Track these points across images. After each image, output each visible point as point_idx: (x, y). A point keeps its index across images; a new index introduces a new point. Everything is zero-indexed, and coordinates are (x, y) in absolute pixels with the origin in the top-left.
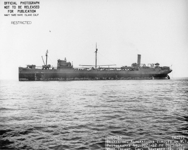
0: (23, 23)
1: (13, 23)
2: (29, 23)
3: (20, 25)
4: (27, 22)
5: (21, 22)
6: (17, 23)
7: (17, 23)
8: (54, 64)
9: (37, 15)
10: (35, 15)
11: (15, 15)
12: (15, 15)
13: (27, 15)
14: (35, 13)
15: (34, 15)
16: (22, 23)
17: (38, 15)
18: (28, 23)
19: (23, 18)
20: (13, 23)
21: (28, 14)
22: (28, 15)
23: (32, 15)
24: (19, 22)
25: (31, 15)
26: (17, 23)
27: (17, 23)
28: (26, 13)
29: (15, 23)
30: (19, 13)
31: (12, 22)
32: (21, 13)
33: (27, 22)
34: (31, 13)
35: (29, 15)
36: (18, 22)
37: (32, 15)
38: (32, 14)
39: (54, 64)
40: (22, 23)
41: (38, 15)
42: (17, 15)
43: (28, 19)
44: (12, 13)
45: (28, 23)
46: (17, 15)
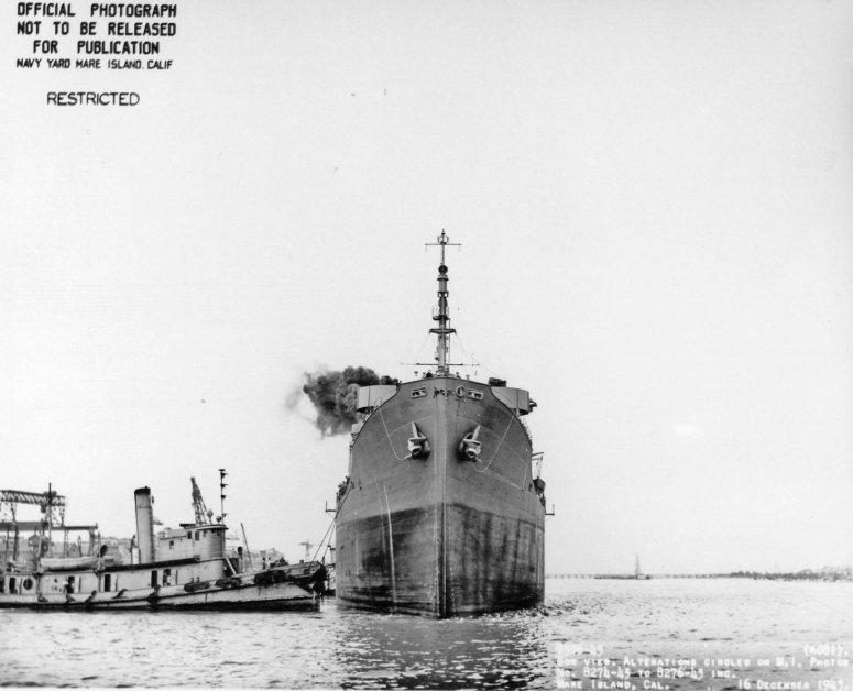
0: (100, 100)
1: (56, 98)
2: (126, 100)
4: (117, 97)
6: (73, 101)
7: (74, 98)
9: (163, 65)
10: (157, 65)
11: (64, 63)
12: (64, 63)
14: (155, 57)
15: (152, 65)
16: (97, 99)
17: (169, 64)
19: (103, 79)
20: (56, 98)
21: (123, 58)
22: (122, 64)
23: (144, 64)
24: (84, 97)
25: (136, 65)
26: (74, 98)
27: (73, 101)
28: (113, 56)
29: (66, 99)
30: (84, 56)
32: (93, 56)
33: (117, 97)
35: (127, 65)
36: (78, 97)
37: (144, 64)
40: (97, 99)
41: (169, 64)
42: (73, 63)
46: (73, 63)
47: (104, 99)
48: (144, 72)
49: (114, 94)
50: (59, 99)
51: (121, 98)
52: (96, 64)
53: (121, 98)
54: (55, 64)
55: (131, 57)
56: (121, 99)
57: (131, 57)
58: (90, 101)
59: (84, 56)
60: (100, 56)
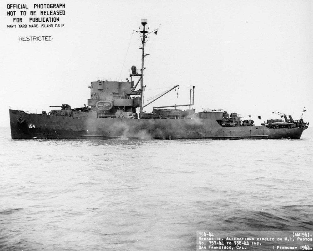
2: (48, 38)
4: (44, 38)
5: (35, 38)
10: (59, 26)
11: (24, 26)
12: (24, 26)
13: (44, 27)
14: (58, 23)
15: (57, 26)
16: (37, 39)
17: (63, 25)
18: (46, 39)
19: (39, 31)
22: (46, 26)
23: (54, 26)
24: (32, 38)
25: (51, 26)
28: (43, 23)
29: (25, 39)
30: (32, 23)
31: (20, 38)
32: (36, 23)
34: (52, 23)
35: (47, 26)
37: (54, 26)
38: (54, 23)
40: (37, 39)
41: (63, 25)
42: (28, 26)
44: (20, 23)
45: (46, 39)
46: (28, 26)
47: (40, 39)
49: (43, 37)
50: (23, 39)
51: (45, 38)
52: (36, 26)
54: (21, 26)
56: (46, 38)
58: (35, 39)
60: (38, 23)
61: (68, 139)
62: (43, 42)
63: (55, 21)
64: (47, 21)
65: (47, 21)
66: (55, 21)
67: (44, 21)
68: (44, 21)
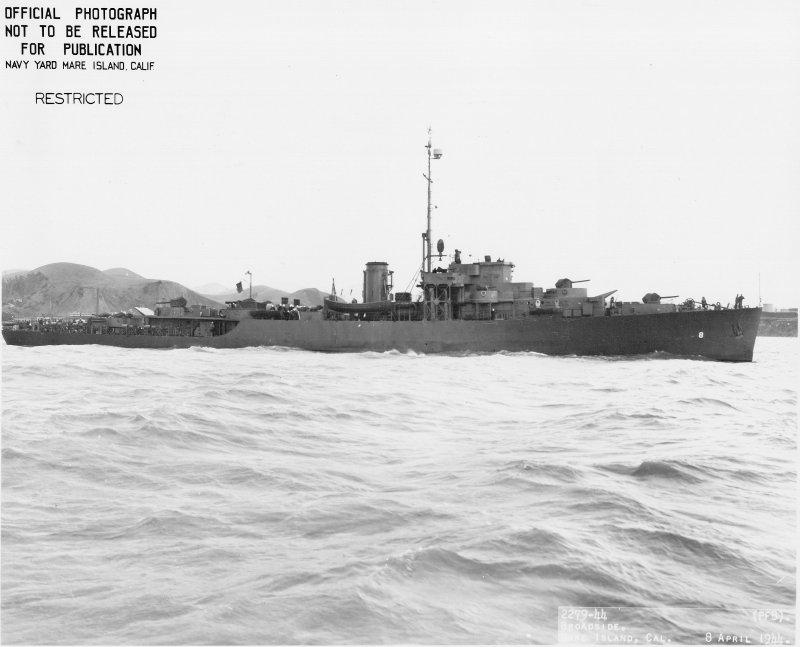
0: (85, 99)
3: (73, 108)
5: (78, 96)
6: (61, 101)
7: (61, 98)
8: (406, 281)
10: (139, 66)
13: (102, 67)
14: (137, 58)
15: (134, 66)
16: (83, 99)
17: (151, 65)
19: (89, 79)
21: (107, 59)
22: (106, 66)
23: (128, 66)
25: (120, 66)
26: (61, 98)
27: (61, 101)
28: (98, 58)
29: (53, 99)
30: (70, 58)
32: (79, 58)
35: (111, 66)
38: (127, 60)
39: (406, 281)
40: (83, 99)
41: (151, 65)
42: (60, 65)
43: (108, 81)
46: (60, 65)
48: (128, 73)
51: (106, 98)
52: (81, 65)
53: (106, 98)
55: (115, 59)
57: (115, 59)
59: (70, 58)
61: (338, 352)
62: (100, 108)
63: (130, 52)
64: (110, 54)
65: (110, 54)
66: (130, 52)
67: (102, 52)
68: (102, 52)
